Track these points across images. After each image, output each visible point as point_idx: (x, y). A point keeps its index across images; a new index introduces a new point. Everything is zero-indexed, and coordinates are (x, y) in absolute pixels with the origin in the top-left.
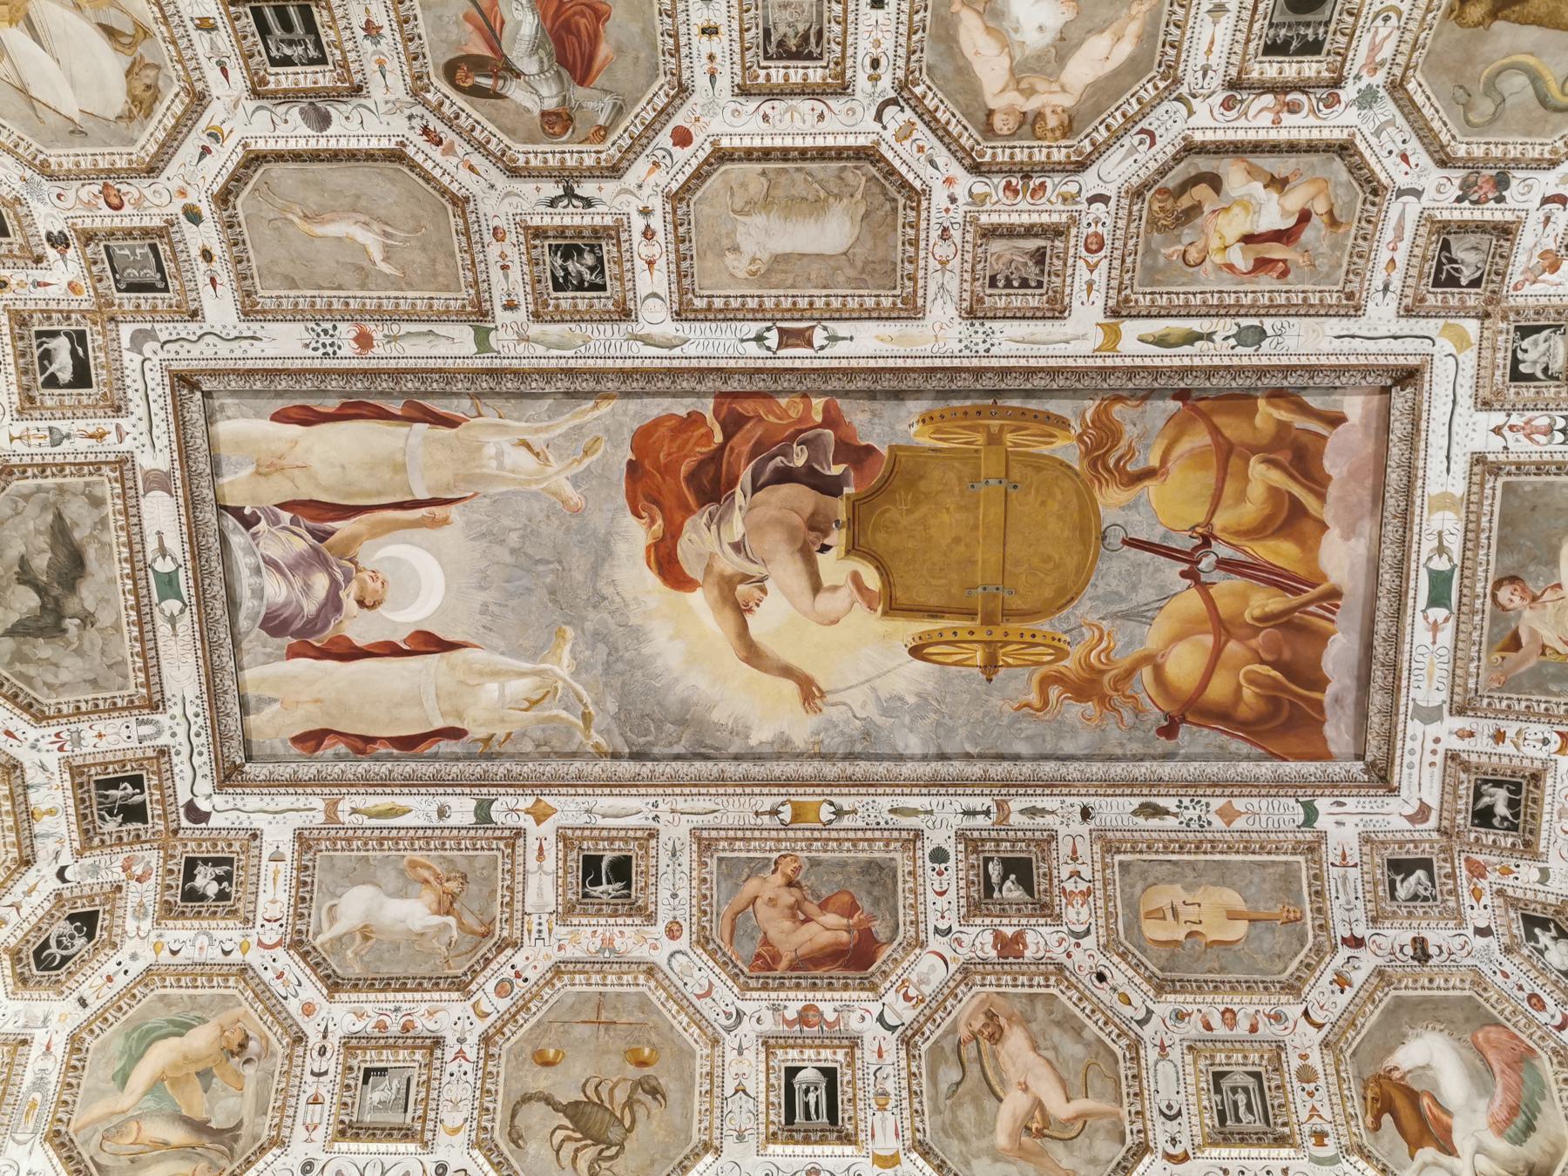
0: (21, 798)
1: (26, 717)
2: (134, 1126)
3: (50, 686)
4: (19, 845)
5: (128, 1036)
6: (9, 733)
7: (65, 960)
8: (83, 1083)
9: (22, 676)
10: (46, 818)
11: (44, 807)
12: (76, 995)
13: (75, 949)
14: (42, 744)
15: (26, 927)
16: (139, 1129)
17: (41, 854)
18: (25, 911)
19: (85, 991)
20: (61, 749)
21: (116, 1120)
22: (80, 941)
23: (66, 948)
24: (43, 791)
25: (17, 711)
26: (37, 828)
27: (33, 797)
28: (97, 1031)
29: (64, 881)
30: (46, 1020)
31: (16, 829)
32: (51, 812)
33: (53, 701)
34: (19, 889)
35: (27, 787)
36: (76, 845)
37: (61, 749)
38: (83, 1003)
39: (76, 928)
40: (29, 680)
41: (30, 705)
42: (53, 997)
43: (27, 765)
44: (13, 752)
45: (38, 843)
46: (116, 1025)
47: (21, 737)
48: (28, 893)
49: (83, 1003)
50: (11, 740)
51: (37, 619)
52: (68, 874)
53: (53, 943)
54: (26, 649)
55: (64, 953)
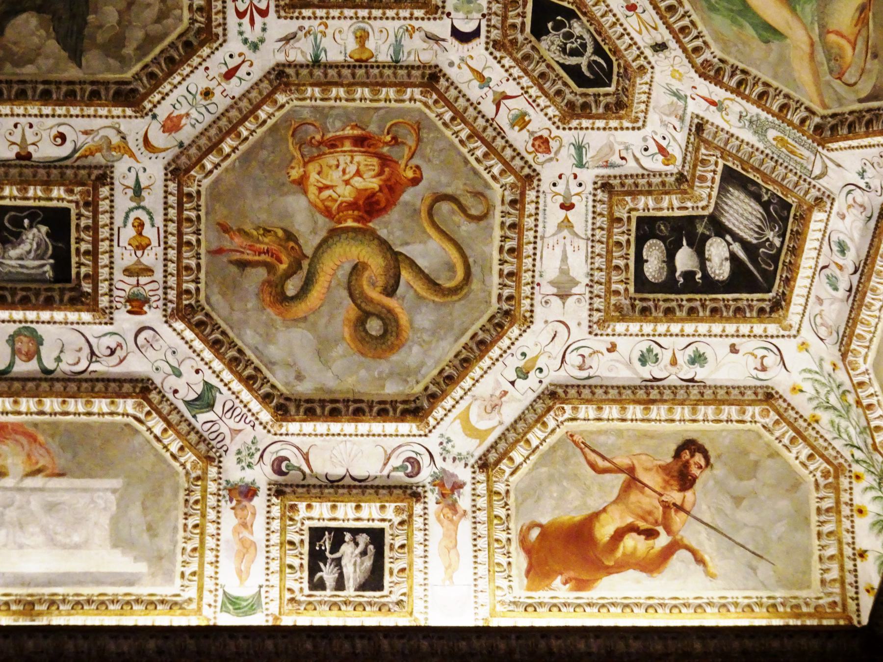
0: (332, 72)
1: (206, 51)
2: (832, 38)
3: (162, 16)
4: (401, 86)
5: (712, 8)
6: (229, 75)
7: (598, 50)
8: (765, 78)
9: (143, 49)
10: (370, 44)
11: (352, 45)
12: (648, 52)
13: (586, 36)
14: (253, 35)
15: (534, 91)
16: (838, 33)
17: (426, 57)
18: (511, 88)
19: (645, 40)
20: (264, 13)
21: (821, 56)
22: (577, 28)
23: (584, 46)
24: (326, 43)
25: (195, 61)
26: (384, 56)
27: (334, 55)
28: (698, 43)
29: (476, 33)
30: (676, 94)
31: (376, 85)
32: (362, 38)
33: (186, 15)
34: (474, 91)
35: (316, 62)
36: (419, 13)
37: (264, 13)
38: (660, 47)
39: (558, 27)
40: (150, 41)
41: (188, 45)
42: (647, 78)
43: (281, 58)
44: (257, 73)
45: (408, 59)
46: (694, 17)
47: (237, 61)
48: (484, 82)
49: (660, 47)
50: (241, 72)
51: (56, 19)
52: (467, 27)
53: (572, 61)
54: (100, 38)
55: (590, 49)
